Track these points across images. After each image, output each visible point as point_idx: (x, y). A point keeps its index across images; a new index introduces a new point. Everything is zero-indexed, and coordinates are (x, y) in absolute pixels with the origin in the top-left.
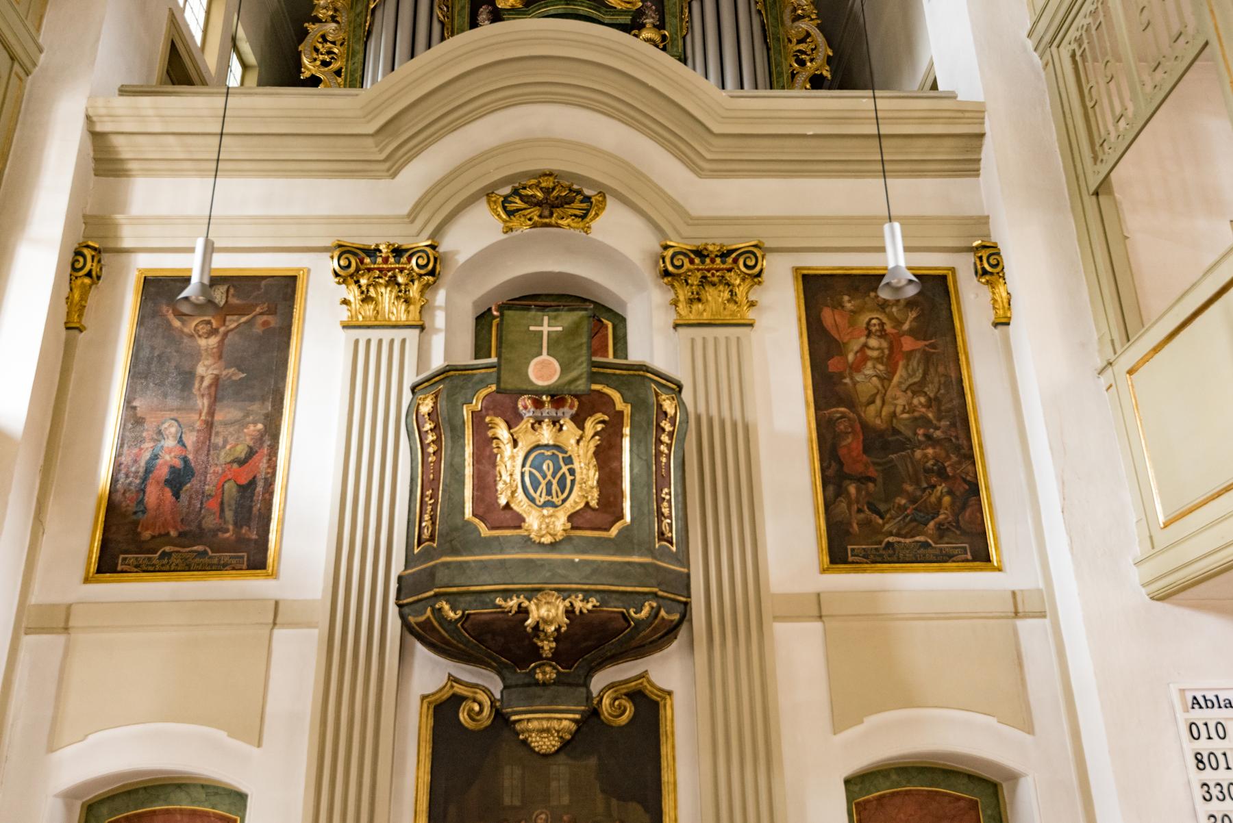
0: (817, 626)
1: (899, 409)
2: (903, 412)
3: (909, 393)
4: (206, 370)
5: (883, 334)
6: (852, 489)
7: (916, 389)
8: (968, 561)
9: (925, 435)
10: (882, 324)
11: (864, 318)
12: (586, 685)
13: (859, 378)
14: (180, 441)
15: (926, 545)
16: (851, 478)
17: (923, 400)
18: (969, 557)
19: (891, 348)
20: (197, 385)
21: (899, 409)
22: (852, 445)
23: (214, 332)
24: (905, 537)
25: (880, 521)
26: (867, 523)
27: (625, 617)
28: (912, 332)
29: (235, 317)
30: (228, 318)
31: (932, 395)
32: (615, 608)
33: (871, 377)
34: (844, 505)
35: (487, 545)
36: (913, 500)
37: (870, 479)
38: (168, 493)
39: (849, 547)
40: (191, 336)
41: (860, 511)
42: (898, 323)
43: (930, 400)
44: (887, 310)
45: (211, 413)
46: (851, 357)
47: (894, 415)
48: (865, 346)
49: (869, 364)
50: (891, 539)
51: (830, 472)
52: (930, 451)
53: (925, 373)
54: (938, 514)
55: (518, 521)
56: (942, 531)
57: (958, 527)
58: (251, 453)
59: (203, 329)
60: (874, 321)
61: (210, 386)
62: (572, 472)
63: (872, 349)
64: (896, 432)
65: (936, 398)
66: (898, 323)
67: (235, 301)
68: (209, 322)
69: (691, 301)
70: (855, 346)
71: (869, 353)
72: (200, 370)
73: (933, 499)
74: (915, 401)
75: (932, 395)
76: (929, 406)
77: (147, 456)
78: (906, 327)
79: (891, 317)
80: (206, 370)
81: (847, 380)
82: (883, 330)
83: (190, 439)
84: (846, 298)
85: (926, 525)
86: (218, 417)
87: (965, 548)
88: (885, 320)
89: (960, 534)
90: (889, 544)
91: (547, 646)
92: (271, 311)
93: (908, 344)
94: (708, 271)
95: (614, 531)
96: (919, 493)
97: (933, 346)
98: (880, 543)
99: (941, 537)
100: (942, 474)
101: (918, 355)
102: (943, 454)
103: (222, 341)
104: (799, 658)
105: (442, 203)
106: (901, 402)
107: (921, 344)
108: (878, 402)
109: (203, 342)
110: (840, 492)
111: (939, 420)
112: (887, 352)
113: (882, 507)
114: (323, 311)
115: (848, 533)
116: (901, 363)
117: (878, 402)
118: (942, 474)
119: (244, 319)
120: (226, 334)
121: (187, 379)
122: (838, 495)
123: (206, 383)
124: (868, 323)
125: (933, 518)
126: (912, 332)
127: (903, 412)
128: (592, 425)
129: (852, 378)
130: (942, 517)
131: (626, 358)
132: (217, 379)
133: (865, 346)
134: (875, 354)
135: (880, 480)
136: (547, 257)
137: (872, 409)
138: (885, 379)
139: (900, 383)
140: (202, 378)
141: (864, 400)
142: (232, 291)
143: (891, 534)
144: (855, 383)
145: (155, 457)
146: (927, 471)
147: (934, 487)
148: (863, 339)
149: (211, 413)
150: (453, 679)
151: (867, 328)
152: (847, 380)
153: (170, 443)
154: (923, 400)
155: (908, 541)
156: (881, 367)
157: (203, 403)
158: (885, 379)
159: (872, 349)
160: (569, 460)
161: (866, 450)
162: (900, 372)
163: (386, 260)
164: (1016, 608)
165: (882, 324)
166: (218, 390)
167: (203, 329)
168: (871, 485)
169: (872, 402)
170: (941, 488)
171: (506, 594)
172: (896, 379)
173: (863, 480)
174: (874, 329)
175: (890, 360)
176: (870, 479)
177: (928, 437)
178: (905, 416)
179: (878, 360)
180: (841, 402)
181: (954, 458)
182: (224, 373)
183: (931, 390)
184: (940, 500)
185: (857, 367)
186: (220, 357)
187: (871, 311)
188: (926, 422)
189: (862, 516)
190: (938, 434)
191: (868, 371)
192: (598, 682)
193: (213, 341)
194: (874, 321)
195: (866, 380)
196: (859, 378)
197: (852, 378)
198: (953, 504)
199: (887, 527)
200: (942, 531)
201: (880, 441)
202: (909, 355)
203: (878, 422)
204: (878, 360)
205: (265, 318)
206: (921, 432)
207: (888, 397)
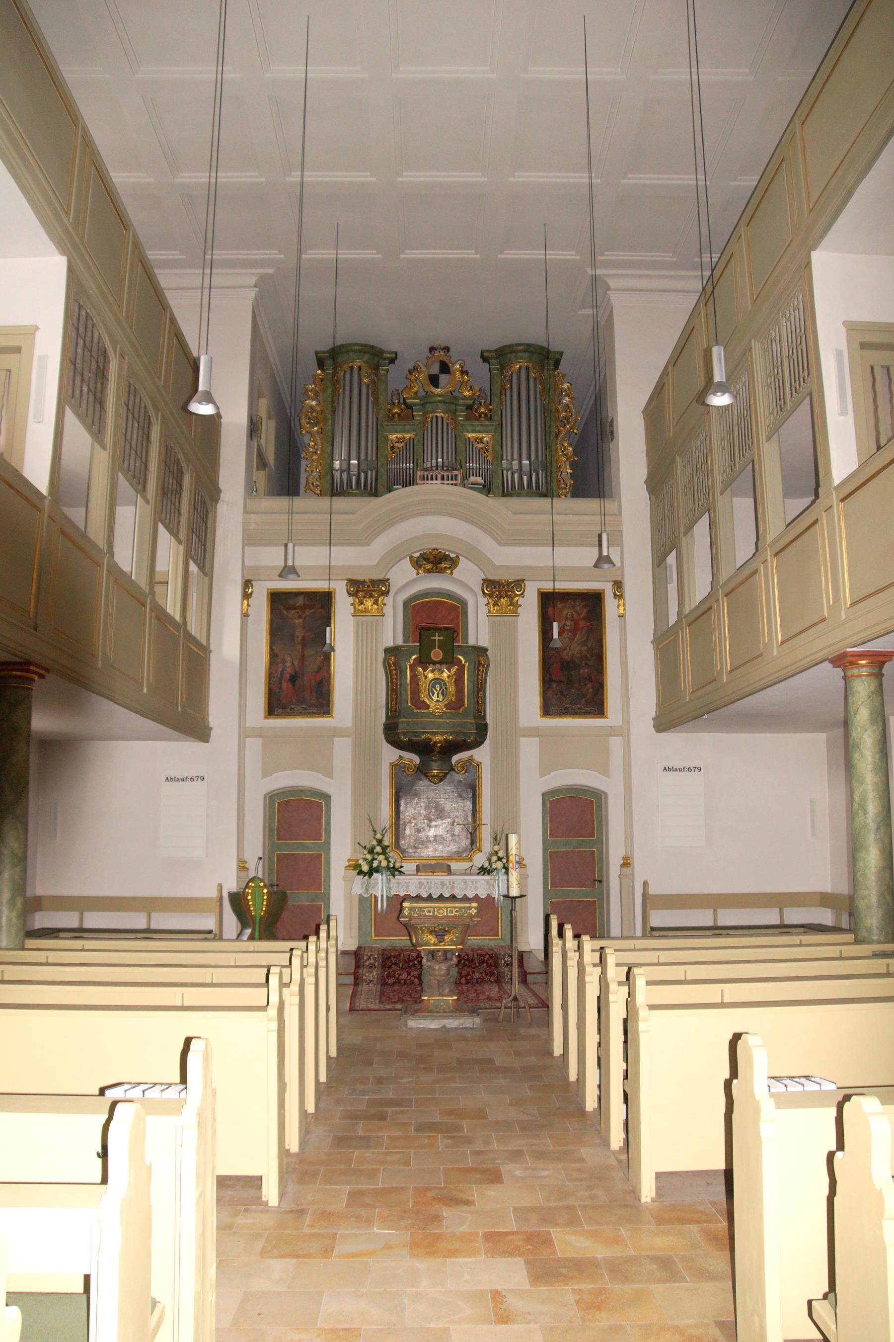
0: (537, 739)
4: (299, 633)
5: (572, 619)
7: (584, 644)
10: (572, 615)
11: (565, 612)
12: (450, 760)
14: (293, 664)
23: (300, 617)
27: (465, 741)
28: (584, 619)
32: (461, 738)
35: (417, 714)
37: (561, 681)
38: (290, 685)
42: (579, 614)
45: (303, 652)
55: (428, 707)
56: (587, 701)
58: (320, 668)
59: (296, 615)
62: (446, 689)
69: (494, 605)
72: (297, 633)
76: (588, 651)
77: (280, 669)
78: (582, 616)
80: (299, 633)
83: (296, 663)
86: (306, 653)
89: (595, 704)
90: (566, 708)
91: (437, 750)
92: (322, 607)
93: (582, 623)
94: (501, 590)
95: (461, 710)
100: (590, 680)
104: (529, 751)
105: (391, 558)
106: (577, 649)
109: (297, 621)
114: (343, 605)
118: (590, 680)
121: (292, 637)
123: (300, 639)
126: (584, 619)
128: (454, 669)
131: (467, 642)
132: (304, 637)
133: (565, 625)
134: (568, 628)
137: (565, 652)
145: (283, 670)
149: (303, 652)
150: (401, 757)
153: (289, 664)
157: (300, 647)
158: (571, 639)
160: (445, 684)
162: (578, 636)
163: (368, 586)
164: (612, 732)
165: (572, 615)
166: (304, 643)
167: (296, 615)
169: (565, 649)
171: (424, 733)
176: (561, 681)
177: (586, 664)
181: (595, 673)
183: (589, 645)
186: (304, 628)
192: (455, 759)
193: (301, 621)
201: (568, 666)
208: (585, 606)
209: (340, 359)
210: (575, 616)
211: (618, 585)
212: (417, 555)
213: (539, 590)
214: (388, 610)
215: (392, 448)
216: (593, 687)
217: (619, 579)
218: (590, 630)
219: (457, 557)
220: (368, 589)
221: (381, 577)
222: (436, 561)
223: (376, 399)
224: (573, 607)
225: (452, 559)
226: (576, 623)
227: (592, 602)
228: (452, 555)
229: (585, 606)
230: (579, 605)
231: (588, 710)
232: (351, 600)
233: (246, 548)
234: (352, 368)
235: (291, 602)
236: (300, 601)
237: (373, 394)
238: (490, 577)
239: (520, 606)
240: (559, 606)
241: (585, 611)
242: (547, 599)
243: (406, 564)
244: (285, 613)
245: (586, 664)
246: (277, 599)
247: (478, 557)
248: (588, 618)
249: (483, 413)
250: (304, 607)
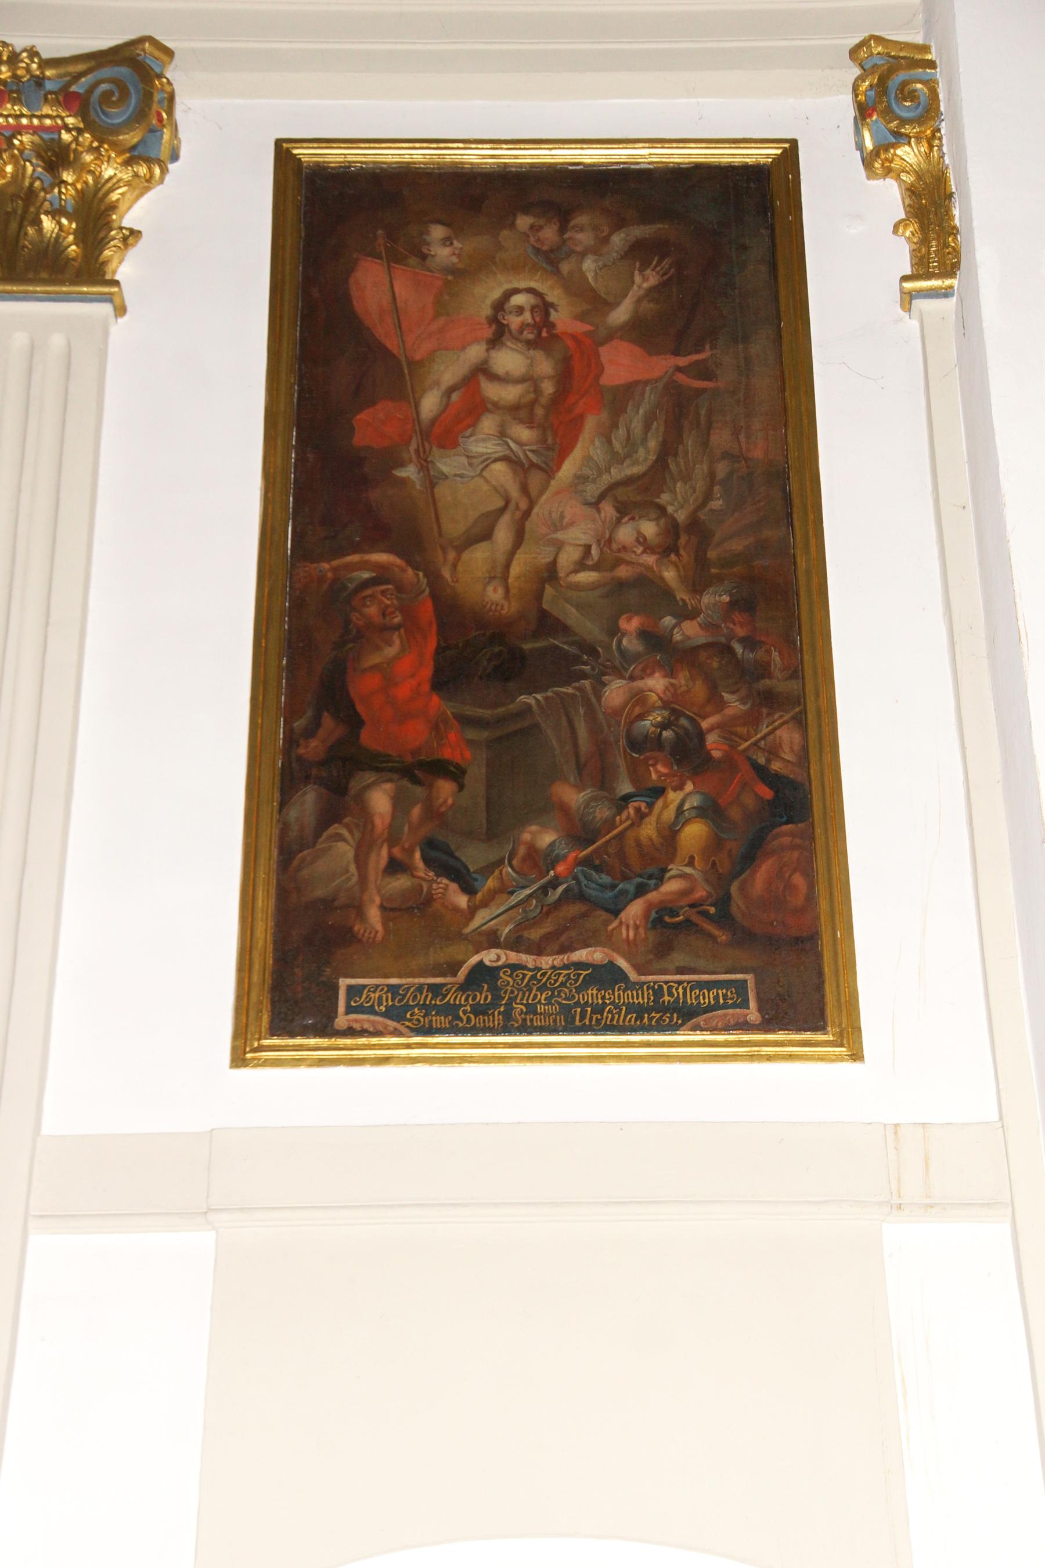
1: (568, 557)
2: (581, 566)
3: (608, 510)
5: (542, 334)
6: (380, 801)
7: (633, 497)
8: (744, 1026)
9: (644, 634)
10: (544, 307)
11: (488, 291)
13: (447, 464)
15: (606, 976)
16: (380, 764)
17: (649, 529)
18: (753, 1014)
19: (565, 376)
21: (568, 557)
22: (396, 669)
24: (538, 950)
25: (462, 901)
26: (417, 907)
28: (642, 332)
31: (681, 516)
33: (488, 461)
34: (345, 850)
36: (582, 833)
37: (456, 774)
39: (344, 983)
41: (395, 867)
42: (597, 304)
43: (673, 530)
44: (565, 268)
46: (430, 404)
47: (550, 573)
48: (483, 370)
49: (488, 424)
50: (489, 957)
51: (313, 748)
52: (656, 683)
53: (667, 452)
54: (660, 877)
56: (668, 929)
57: (724, 917)
60: (518, 300)
64: (547, 623)
65: (694, 525)
66: (597, 304)
70: (449, 371)
71: (492, 391)
73: (648, 830)
74: (625, 534)
75: (681, 516)
76: (667, 549)
78: (621, 314)
81: (409, 472)
82: (545, 323)
84: (438, 232)
85: (616, 913)
87: (741, 987)
88: (554, 295)
90: (482, 974)
93: (620, 364)
96: (602, 812)
97: (704, 372)
98: (453, 968)
99: (663, 949)
100: (688, 753)
101: (650, 397)
102: (699, 690)
106: (579, 534)
107: (663, 365)
108: (503, 535)
110: (339, 805)
111: (697, 587)
112: (548, 388)
113: (473, 856)
115: (345, 937)
116: (590, 423)
117: (503, 535)
122: (330, 816)
124: (500, 306)
125: (641, 891)
126: (642, 332)
127: (581, 566)
129: (425, 465)
130: (671, 886)
133: (483, 370)
134: (510, 394)
135: (477, 773)
137: (479, 556)
138: (533, 469)
139: (580, 479)
141: (455, 526)
143: (492, 940)
144: (432, 482)
146: (636, 744)
147: (659, 792)
148: (475, 352)
151: (494, 320)
152: (409, 472)
154: (649, 529)
155: (546, 962)
156: (525, 434)
158: (533, 469)
159: (493, 377)
161: (448, 677)
162: (586, 450)
165: (544, 307)
168: (445, 788)
170: (684, 796)
172: (568, 469)
173: (420, 770)
174: (514, 321)
175: (556, 418)
177: (655, 641)
178: (585, 577)
180: (379, 533)
181: (735, 705)
184: (670, 835)
185: (447, 433)
187: (516, 268)
188: (648, 593)
189: (401, 883)
190: (690, 632)
191: (483, 441)
194: (518, 300)
195: (473, 472)
196: (447, 464)
197: (425, 465)
198: (715, 844)
199: (481, 918)
200: (668, 929)
201: (495, 657)
202: (621, 398)
203: (494, 594)
206: (631, 625)
207: (525, 510)
210: (563, 318)
211: (897, 91)
213: (284, 153)
216: (711, 811)
218: (679, 410)
224: (550, 259)
227: (718, 239)
229: (640, 252)
230: (597, 254)
231: (671, 981)
239: (135, 234)
240: (442, 254)
242: (338, 219)
245: (655, 641)
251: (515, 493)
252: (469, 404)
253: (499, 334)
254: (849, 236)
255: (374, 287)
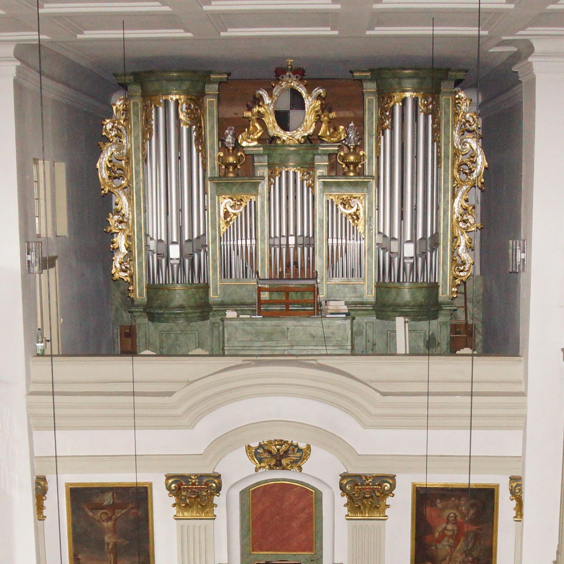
3: (464, 555)
5: (455, 522)
10: (456, 517)
11: (447, 513)
13: (440, 546)
17: (470, 559)
20: (106, 548)
23: (109, 519)
29: (119, 510)
30: (116, 511)
33: (446, 546)
40: (99, 521)
42: (464, 515)
46: (437, 535)
48: (445, 529)
49: (446, 539)
59: (104, 517)
60: (451, 515)
61: (112, 549)
63: (448, 530)
67: (117, 501)
68: (106, 513)
70: (440, 529)
71: (446, 532)
72: (107, 539)
79: (461, 512)
80: (109, 539)
81: (433, 548)
84: (438, 501)
92: (138, 507)
93: (468, 528)
97: (481, 529)
101: (472, 534)
103: (114, 524)
105: (222, 444)
107: (473, 528)
108: (448, 559)
109: (105, 524)
112: (456, 532)
114: (162, 506)
117: (448, 559)
119: (124, 511)
120: (116, 519)
123: (110, 547)
124: (449, 515)
132: (115, 544)
133: (445, 529)
134: (449, 533)
136: (279, 475)
140: (108, 544)
142: (115, 495)
144: (436, 548)
148: (444, 525)
151: (447, 519)
152: (433, 548)
156: (452, 541)
158: (453, 547)
159: (448, 530)
165: (456, 517)
166: (117, 551)
167: (104, 517)
172: (459, 547)
174: (451, 519)
175: (456, 538)
179: (451, 537)
182: (119, 541)
183: (475, 554)
185: (439, 541)
187: (452, 508)
191: (445, 543)
193: (110, 524)
194: (451, 515)
196: (440, 546)
204: (451, 537)
205: (135, 511)
208: (472, 506)
209: (153, 86)
210: (459, 518)
212: (255, 445)
213: (414, 485)
214: (220, 511)
215: (227, 214)
217: (517, 474)
218: (477, 537)
219: (309, 447)
220: (195, 493)
221: (209, 471)
222: (280, 454)
223: (205, 158)
224: (457, 507)
225: (300, 450)
226: (460, 527)
228: (302, 445)
229: (472, 506)
232: (173, 500)
233: (35, 433)
234: (166, 103)
235: (97, 500)
236: (108, 499)
237: (197, 139)
238: (352, 471)
240: (439, 505)
241: (472, 512)
243: (241, 454)
244: (91, 514)
246: (80, 496)
247: (333, 442)
248: (475, 521)
249: (352, 163)
250: (113, 507)
251: (450, 552)
252: (443, 535)
253: (447, 523)
254: (505, 505)
255: (429, 512)
